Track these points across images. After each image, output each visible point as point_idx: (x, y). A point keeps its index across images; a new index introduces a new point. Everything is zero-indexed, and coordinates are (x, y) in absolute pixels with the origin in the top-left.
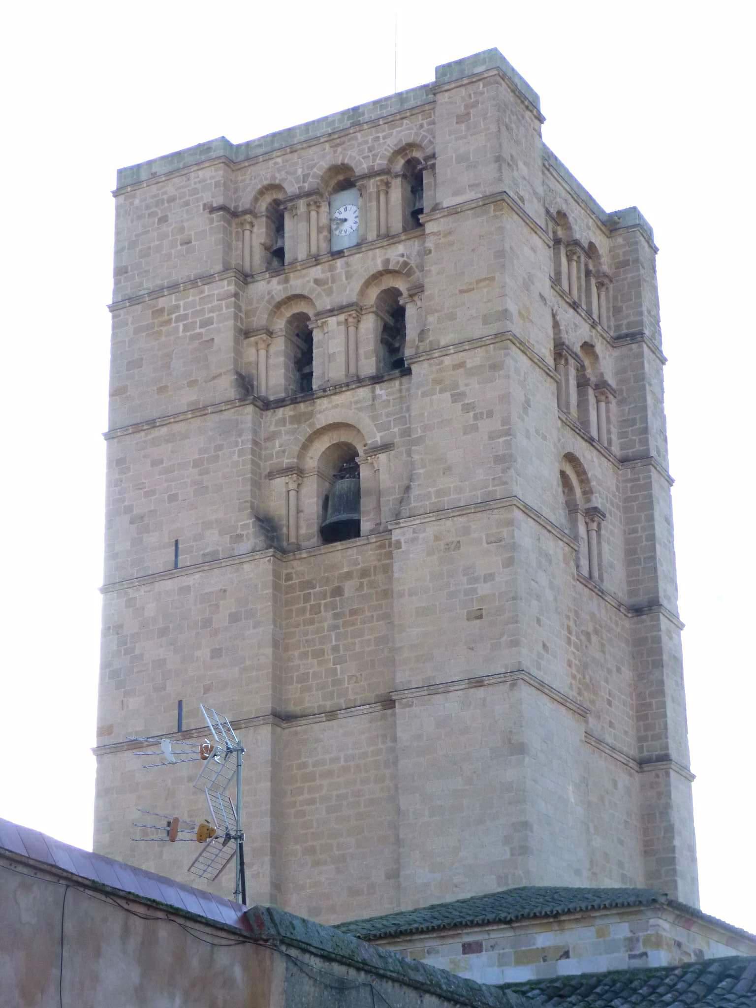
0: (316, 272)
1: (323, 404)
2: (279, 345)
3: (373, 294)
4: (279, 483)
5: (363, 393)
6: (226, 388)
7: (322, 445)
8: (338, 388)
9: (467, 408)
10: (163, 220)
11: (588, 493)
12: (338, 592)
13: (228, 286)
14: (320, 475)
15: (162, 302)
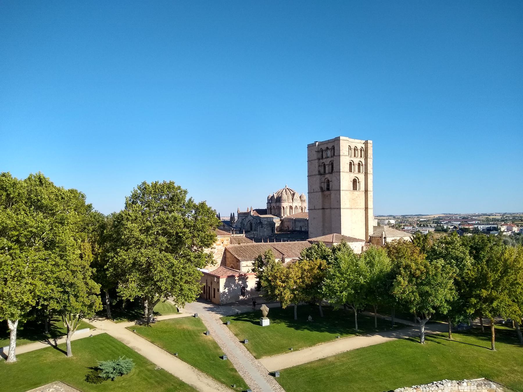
0: (325, 160)
1: (326, 175)
2: (323, 167)
3: (331, 163)
4: (322, 183)
5: (329, 175)
6: (317, 173)
7: (327, 179)
8: (327, 174)
9: (337, 179)
10: (311, 152)
11: (358, 180)
12: (327, 196)
13: (317, 161)
14: (326, 182)
15: (312, 162)
